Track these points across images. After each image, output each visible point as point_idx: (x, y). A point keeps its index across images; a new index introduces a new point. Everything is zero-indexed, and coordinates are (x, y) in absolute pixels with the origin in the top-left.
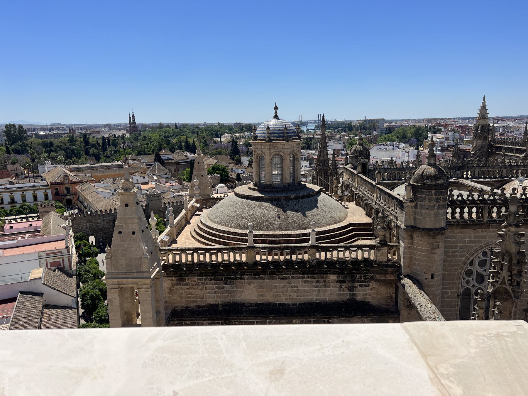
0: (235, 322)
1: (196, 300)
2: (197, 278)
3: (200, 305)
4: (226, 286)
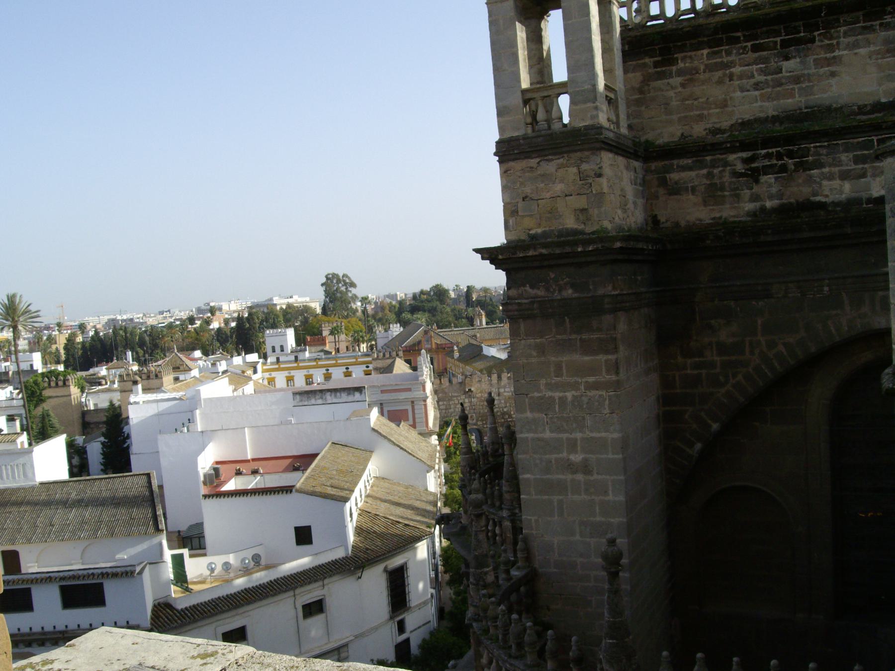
0: (816, 147)
1: (705, 112)
2: (705, 52)
3: (718, 126)
4: (787, 65)
